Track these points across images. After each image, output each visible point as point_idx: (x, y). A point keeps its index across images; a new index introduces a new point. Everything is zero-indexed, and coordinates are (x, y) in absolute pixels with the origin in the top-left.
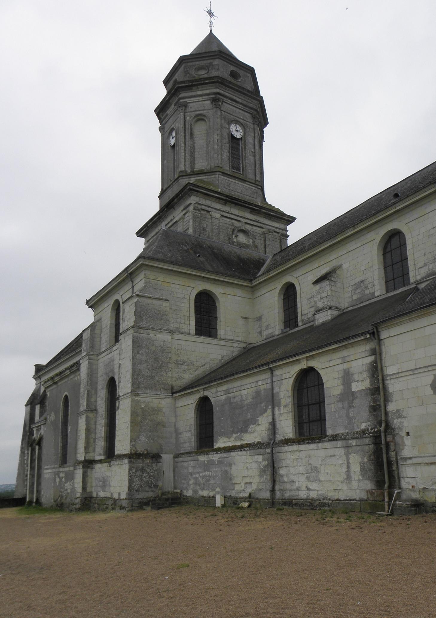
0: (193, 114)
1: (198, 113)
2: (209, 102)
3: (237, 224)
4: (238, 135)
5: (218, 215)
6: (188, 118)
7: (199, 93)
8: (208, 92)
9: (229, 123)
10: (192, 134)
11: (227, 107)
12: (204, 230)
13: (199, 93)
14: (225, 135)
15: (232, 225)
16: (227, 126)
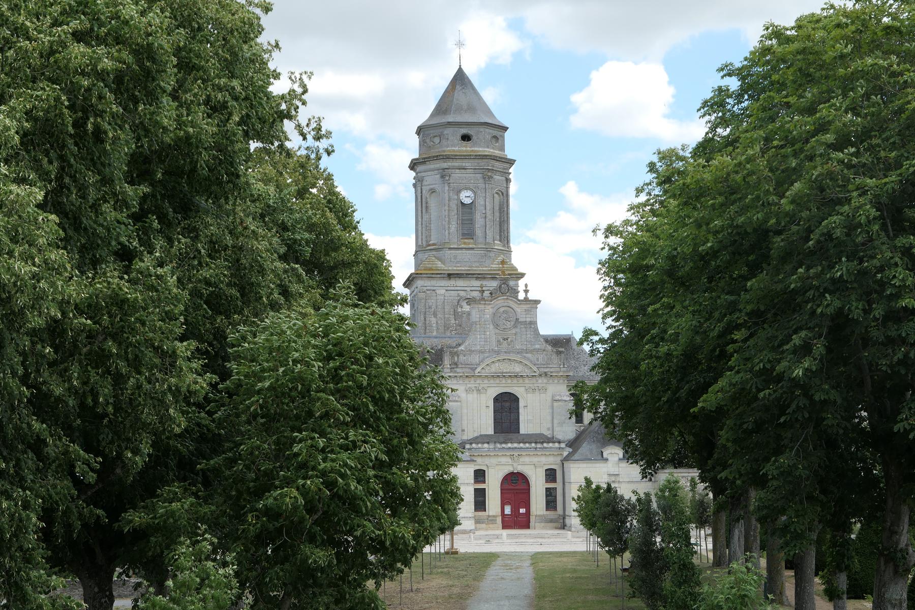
0: (428, 187)
1: (432, 187)
2: (438, 176)
3: (462, 294)
4: (467, 201)
5: (442, 291)
6: (424, 192)
7: (432, 166)
8: (438, 166)
9: (459, 192)
10: (427, 207)
11: (457, 175)
12: (430, 307)
13: (432, 166)
14: (454, 207)
15: (458, 295)
16: (456, 197)
